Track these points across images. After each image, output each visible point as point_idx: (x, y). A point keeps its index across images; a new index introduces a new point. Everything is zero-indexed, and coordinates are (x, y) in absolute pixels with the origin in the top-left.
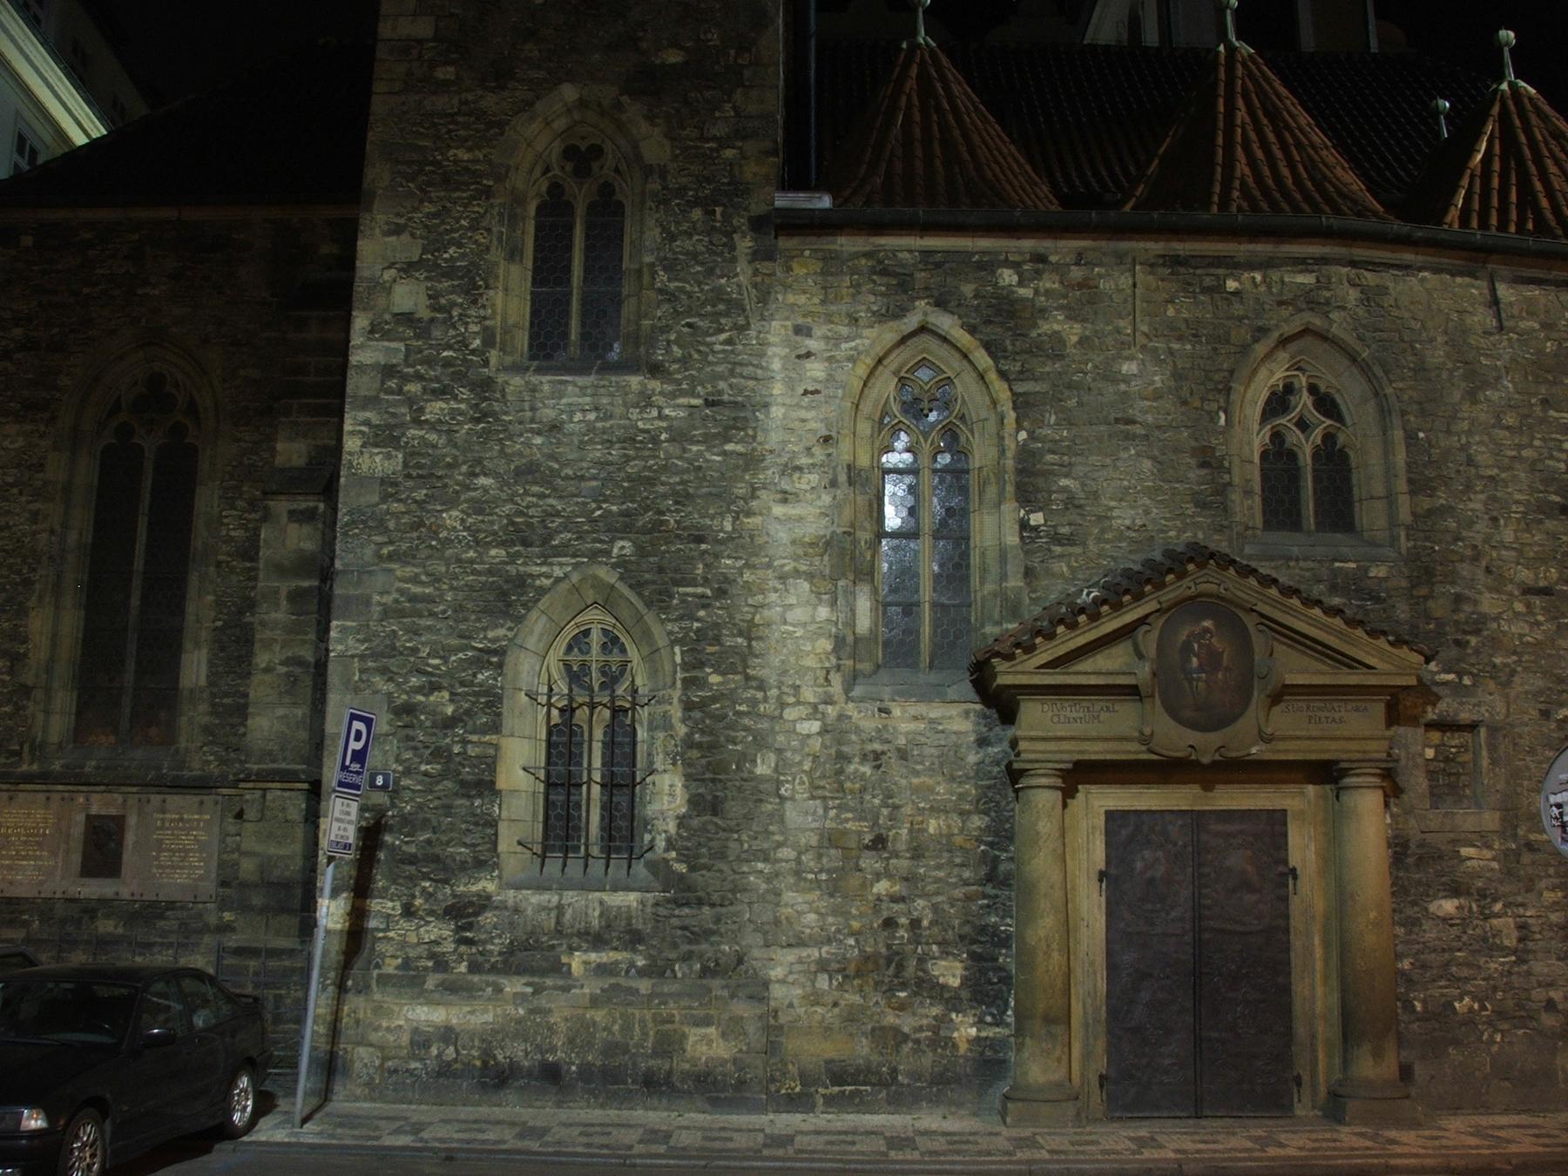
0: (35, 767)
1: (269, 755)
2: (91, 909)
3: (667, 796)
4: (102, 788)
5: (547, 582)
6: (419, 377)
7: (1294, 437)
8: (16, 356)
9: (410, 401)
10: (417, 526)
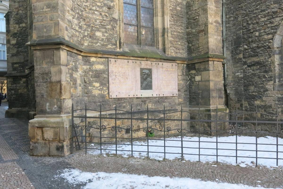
0: (121, 50)
2: (144, 100)
4: (145, 59)
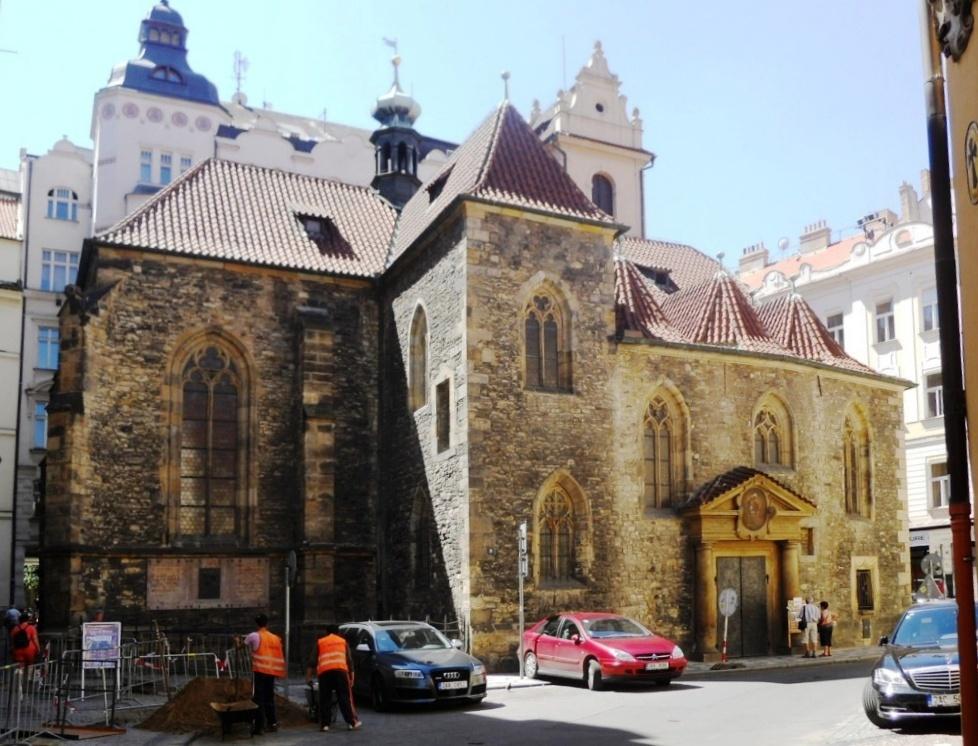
1: (316, 538)
3: (588, 554)
5: (545, 475)
6: (495, 390)
7: (764, 429)
8: (139, 332)
9: (492, 400)
10: (499, 450)
